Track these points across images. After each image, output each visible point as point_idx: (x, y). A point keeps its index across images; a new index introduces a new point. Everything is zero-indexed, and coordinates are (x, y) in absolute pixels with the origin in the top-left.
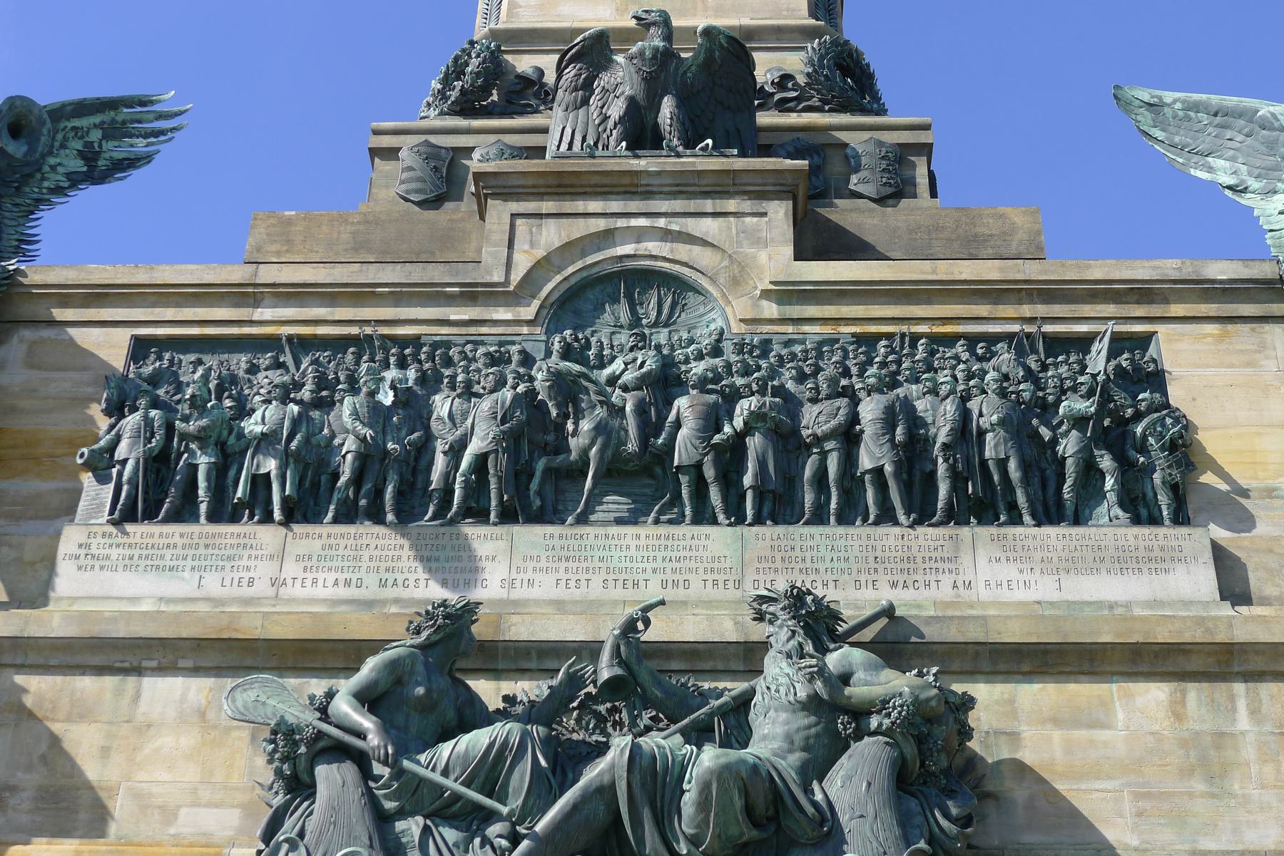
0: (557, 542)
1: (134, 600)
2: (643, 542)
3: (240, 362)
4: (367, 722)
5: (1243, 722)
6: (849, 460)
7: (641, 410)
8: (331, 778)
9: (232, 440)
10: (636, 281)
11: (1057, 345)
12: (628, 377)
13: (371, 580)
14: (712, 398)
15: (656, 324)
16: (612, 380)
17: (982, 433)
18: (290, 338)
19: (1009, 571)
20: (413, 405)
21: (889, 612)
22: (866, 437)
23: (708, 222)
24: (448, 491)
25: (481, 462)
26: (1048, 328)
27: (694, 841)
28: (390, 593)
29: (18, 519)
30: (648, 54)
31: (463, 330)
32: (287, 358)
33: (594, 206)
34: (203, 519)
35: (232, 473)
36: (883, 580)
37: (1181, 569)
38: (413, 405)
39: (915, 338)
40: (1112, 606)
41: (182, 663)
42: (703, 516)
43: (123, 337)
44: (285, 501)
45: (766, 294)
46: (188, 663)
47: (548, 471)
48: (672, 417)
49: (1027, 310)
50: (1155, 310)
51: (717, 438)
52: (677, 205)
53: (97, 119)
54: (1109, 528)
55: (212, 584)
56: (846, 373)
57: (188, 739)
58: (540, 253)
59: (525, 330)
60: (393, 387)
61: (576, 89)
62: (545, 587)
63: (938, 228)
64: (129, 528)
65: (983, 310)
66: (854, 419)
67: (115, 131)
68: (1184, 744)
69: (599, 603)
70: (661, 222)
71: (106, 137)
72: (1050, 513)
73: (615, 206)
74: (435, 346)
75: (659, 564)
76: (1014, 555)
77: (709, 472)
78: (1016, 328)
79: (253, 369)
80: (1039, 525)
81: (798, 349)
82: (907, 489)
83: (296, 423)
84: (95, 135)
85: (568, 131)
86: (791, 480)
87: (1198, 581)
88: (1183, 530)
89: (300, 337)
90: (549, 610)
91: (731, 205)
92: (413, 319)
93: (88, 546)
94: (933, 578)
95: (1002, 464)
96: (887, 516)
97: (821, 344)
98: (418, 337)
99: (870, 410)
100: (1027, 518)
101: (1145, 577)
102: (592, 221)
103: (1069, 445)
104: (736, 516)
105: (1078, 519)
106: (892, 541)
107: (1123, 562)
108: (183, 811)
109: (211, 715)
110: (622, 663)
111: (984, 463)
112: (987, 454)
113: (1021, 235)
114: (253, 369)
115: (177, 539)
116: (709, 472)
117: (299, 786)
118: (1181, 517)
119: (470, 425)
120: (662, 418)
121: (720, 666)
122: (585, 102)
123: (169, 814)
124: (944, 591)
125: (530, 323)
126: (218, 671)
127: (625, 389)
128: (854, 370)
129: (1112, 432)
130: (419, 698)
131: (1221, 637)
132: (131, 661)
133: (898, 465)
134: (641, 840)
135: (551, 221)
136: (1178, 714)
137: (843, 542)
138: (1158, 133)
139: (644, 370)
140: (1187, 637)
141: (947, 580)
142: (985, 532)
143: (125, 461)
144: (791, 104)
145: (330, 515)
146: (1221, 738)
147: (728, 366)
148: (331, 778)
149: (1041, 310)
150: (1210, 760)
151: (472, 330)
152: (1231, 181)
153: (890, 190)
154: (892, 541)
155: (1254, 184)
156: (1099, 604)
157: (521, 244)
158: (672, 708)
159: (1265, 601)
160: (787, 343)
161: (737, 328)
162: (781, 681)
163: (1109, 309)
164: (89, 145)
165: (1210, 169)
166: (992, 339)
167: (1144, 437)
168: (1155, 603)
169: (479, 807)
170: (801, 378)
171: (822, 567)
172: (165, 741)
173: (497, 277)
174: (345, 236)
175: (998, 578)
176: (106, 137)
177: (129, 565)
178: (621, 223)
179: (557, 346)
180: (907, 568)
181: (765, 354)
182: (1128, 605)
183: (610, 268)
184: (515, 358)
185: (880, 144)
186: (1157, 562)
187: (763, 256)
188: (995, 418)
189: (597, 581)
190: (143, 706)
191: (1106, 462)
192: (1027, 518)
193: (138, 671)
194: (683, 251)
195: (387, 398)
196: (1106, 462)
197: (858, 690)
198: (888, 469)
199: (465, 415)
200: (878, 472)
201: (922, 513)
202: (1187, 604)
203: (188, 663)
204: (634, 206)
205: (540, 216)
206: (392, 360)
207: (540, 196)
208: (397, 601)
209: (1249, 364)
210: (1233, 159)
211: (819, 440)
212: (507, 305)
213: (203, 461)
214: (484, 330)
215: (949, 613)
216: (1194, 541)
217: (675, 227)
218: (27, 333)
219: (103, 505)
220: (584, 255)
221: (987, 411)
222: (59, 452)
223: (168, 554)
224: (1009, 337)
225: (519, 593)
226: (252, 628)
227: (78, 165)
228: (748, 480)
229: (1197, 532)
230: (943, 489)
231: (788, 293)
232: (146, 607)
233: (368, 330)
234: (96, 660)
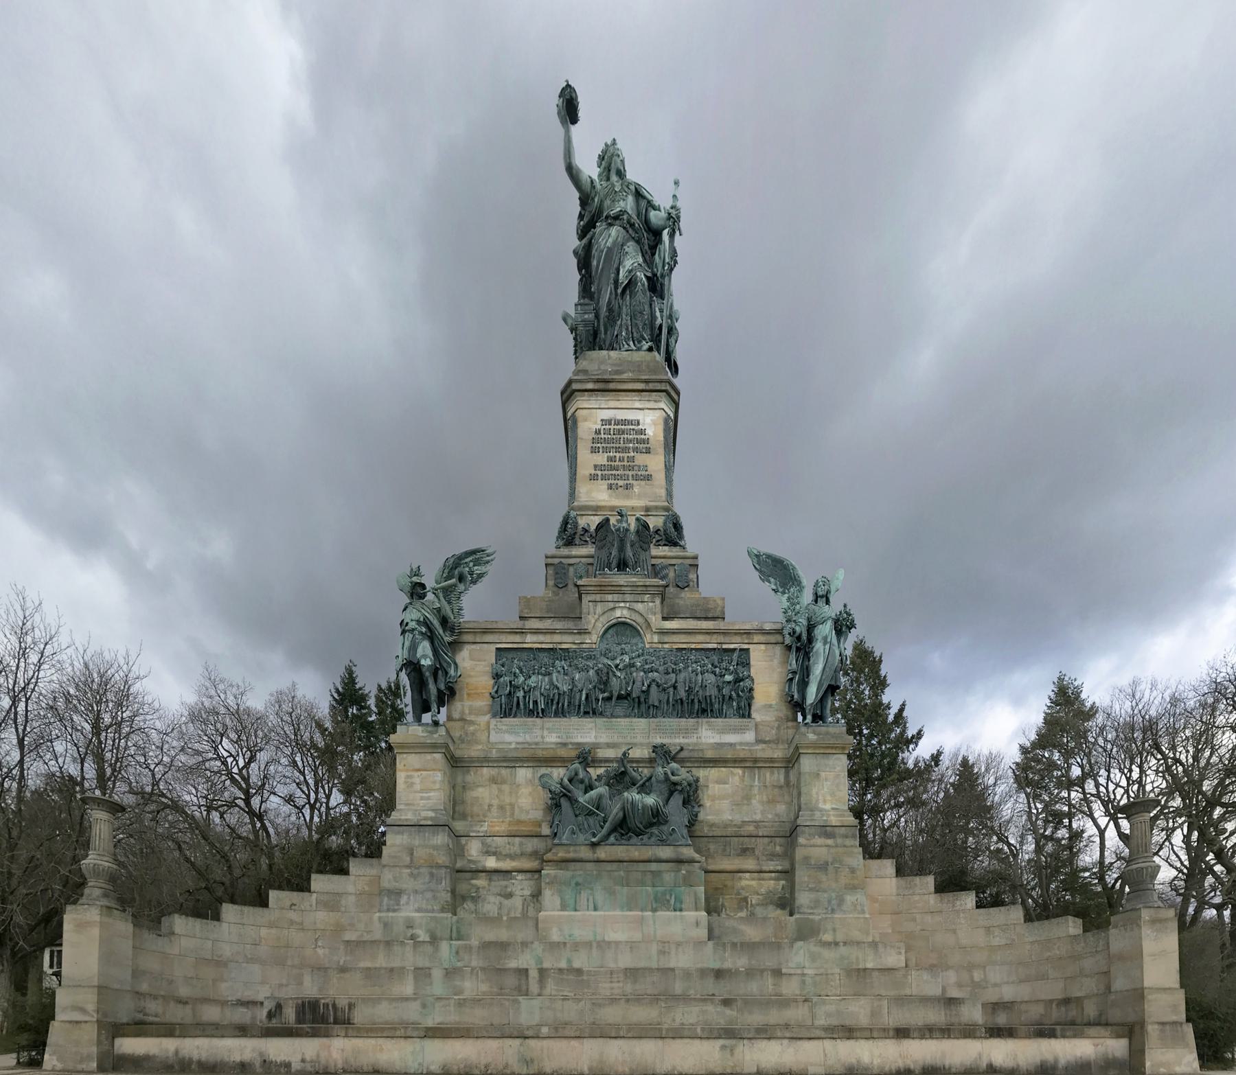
16: (617, 666)
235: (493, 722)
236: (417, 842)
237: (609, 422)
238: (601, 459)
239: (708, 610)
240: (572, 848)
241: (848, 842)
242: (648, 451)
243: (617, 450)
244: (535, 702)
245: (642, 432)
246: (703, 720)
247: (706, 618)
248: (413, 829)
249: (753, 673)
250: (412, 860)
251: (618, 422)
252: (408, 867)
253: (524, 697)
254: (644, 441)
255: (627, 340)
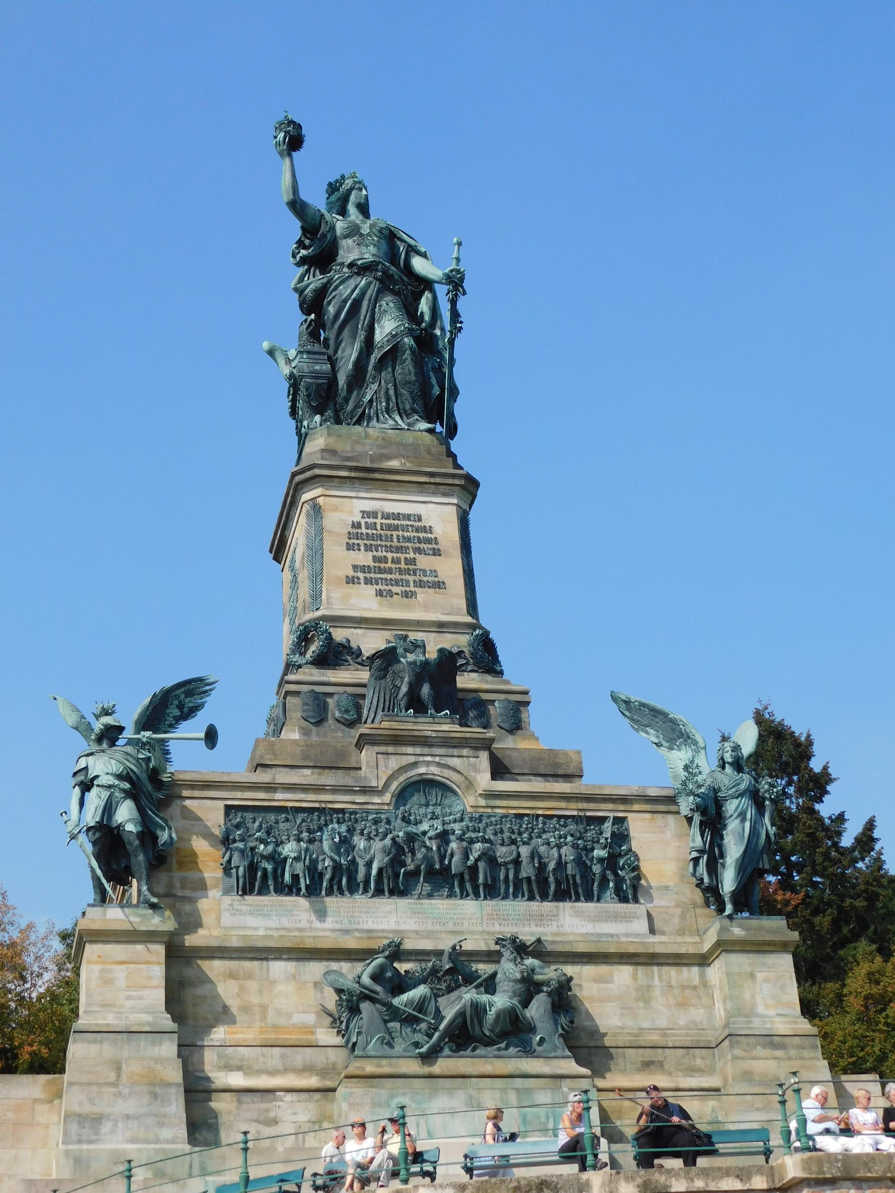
0: (412, 906)
1: (256, 929)
2: (445, 906)
3: (272, 817)
4: (378, 988)
5: (656, 981)
6: (517, 871)
7: (439, 849)
8: (365, 1006)
9: (276, 857)
10: (426, 784)
11: (592, 820)
12: (431, 833)
13: (346, 921)
14: (465, 844)
15: (435, 805)
16: (424, 833)
17: (566, 863)
18: (291, 808)
19: (577, 921)
20: (345, 843)
21: (539, 941)
22: (524, 863)
23: (456, 759)
24: (367, 883)
25: (380, 871)
26: (588, 814)
27: (491, 1031)
28: (354, 927)
29: (196, 890)
30: (418, 663)
31: (361, 807)
32: (290, 817)
33: (410, 750)
34: (272, 892)
35: (279, 871)
36: (533, 923)
37: (636, 920)
38: (345, 843)
39: (538, 816)
40: (612, 935)
41: (283, 957)
42: (464, 895)
43: (221, 805)
44: (306, 885)
45: (481, 795)
46: (286, 957)
47: (405, 873)
48: (449, 852)
49: (580, 805)
50: (628, 808)
51: (469, 863)
52: (442, 751)
53: (183, 690)
54: (610, 905)
55: (285, 922)
56: (513, 832)
57: (290, 988)
58: (390, 772)
59: (386, 807)
60: (339, 834)
61: (381, 670)
62: (409, 925)
63: (542, 759)
64: (246, 897)
65: (563, 804)
66: (519, 855)
67: (190, 694)
68: (637, 989)
69: (432, 932)
70: (437, 759)
71: (186, 697)
72: (589, 898)
73: (418, 750)
74: (351, 813)
75: (452, 916)
76: (578, 914)
77: (467, 877)
78: (575, 813)
79: (277, 822)
80: (587, 901)
81: (493, 819)
82: (538, 883)
83: (307, 850)
84: (182, 696)
85: (377, 689)
86: (495, 879)
87: (642, 926)
88: (637, 905)
89: (295, 808)
90: (414, 935)
91: (465, 752)
92: (342, 801)
93: (232, 905)
94: (549, 923)
95: (574, 877)
96: (531, 898)
97: (502, 817)
98: (343, 809)
99: (524, 851)
100: (582, 899)
101: (624, 923)
102: (409, 757)
103: (597, 869)
104: (477, 895)
105: (598, 900)
106: (535, 908)
107: (616, 918)
108: (294, 1015)
109: (297, 978)
110: (453, 962)
111: (567, 876)
112: (569, 872)
113: (574, 764)
114: (277, 822)
115: (267, 902)
116: (467, 877)
117: (354, 1010)
118: (636, 901)
119: (373, 852)
120: (446, 851)
121: (479, 959)
122: (384, 677)
123: (289, 1016)
124: (554, 928)
125: (387, 804)
126: (298, 959)
127: (430, 838)
128: (516, 831)
129: (611, 862)
130: (389, 977)
131: (651, 951)
132: (264, 955)
133: (536, 875)
134: (473, 1030)
135: (393, 756)
136: (635, 977)
137: (517, 908)
138: (627, 713)
139: (438, 831)
140: (639, 951)
141: (555, 923)
142: (568, 905)
143: (237, 868)
144: (463, 668)
145: (323, 893)
146: (649, 988)
147: (468, 827)
148: (365, 1006)
149: (585, 805)
150: (644, 995)
151: (365, 807)
152: (656, 741)
153: (515, 726)
154: (535, 908)
155: (664, 743)
156: (607, 935)
157: (382, 767)
158: (470, 979)
159: (663, 933)
160: (489, 817)
161: (469, 809)
162: (509, 969)
163: (610, 806)
164: (180, 702)
165: (647, 733)
166: (566, 817)
167: (623, 865)
168: (627, 935)
169: (416, 1017)
170: (495, 834)
171: (510, 918)
172: (281, 988)
173: (374, 784)
174: (299, 752)
175: (571, 923)
176: (186, 697)
177: (251, 913)
178: (421, 759)
179: (400, 816)
180: (541, 919)
181: (481, 821)
182: (617, 935)
183: (416, 778)
184: (385, 821)
185: (509, 702)
186: (628, 918)
187: (479, 777)
188: (572, 858)
189: (430, 922)
190: (271, 974)
191: (611, 877)
192: (582, 899)
193: (267, 959)
194: (447, 773)
195: (337, 840)
196: (611, 877)
197: (538, 977)
198: (533, 878)
199: (370, 848)
200: (529, 879)
201: (544, 897)
202: (638, 935)
203: (286, 957)
204: (426, 750)
205: (388, 754)
206: (335, 820)
207: (387, 744)
208: (357, 930)
209: (662, 832)
210: (657, 731)
211: (506, 864)
212: (379, 796)
213: (269, 867)
214: (370, 807)
215: (558, 939)
216: (640, 909)
217: (442, 762)
218: (178, 802)
219: (233, 886)
220: (406, 772)
221: (568, 854)
222: (205, 859)
223: (265, 909)
224: (573, 817)
225: (403, 927)
226: (309, 944)
227: (177, 712)
228: (481, 880)
229: (642, 907)
230: (553, 887)
231: (490, 795)
232: (261, 932)
233: (323, 805)
234: (250, 955)
235: (227, 900)
236: (125, 1054)
237: (374, 515)
238: (365, 558)
239: (557, 765)
240: (384, 1062)
241: (806, 1054)
242: (437, 553)
243: (389, 549)
244: (295, 877)
245: (430, 530)
246: (566, 907)
247: (556, 776)
248: (119, 1036)
249: (635, 846)
250: (118, 1076)
251: (387, 516)
252: (114, 1084)
253: (275, 870)
254: (428, 541)
255: (388, 411)
